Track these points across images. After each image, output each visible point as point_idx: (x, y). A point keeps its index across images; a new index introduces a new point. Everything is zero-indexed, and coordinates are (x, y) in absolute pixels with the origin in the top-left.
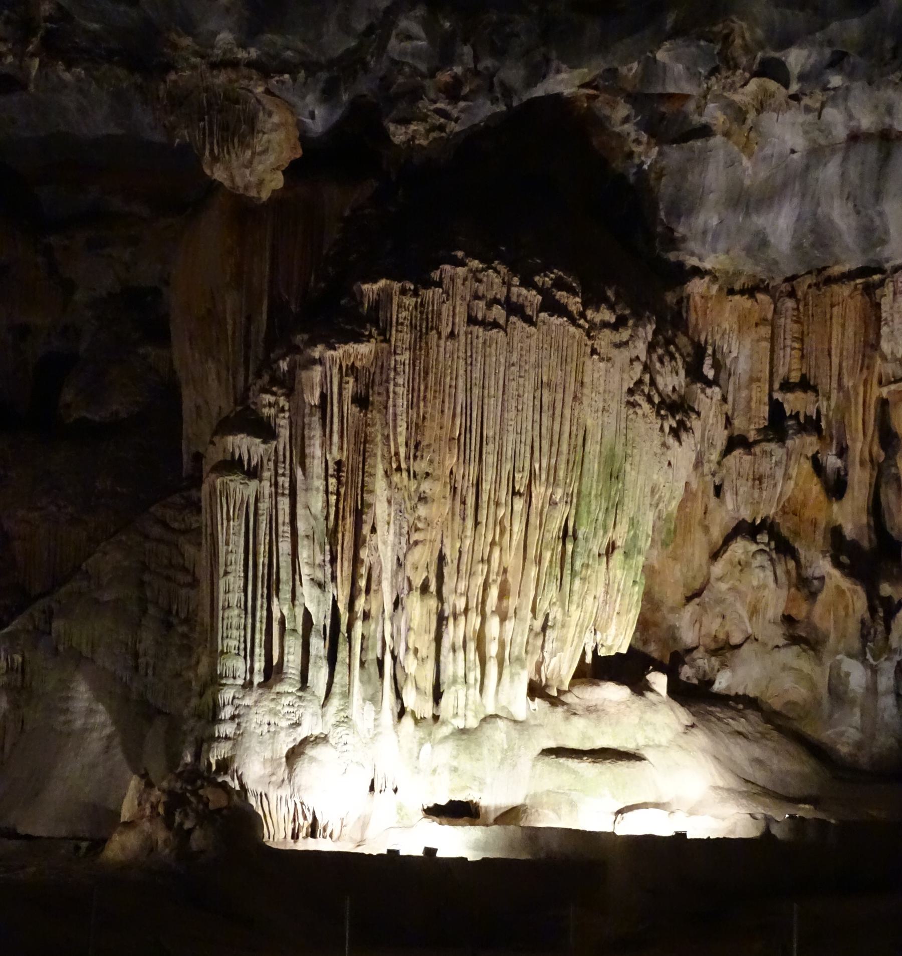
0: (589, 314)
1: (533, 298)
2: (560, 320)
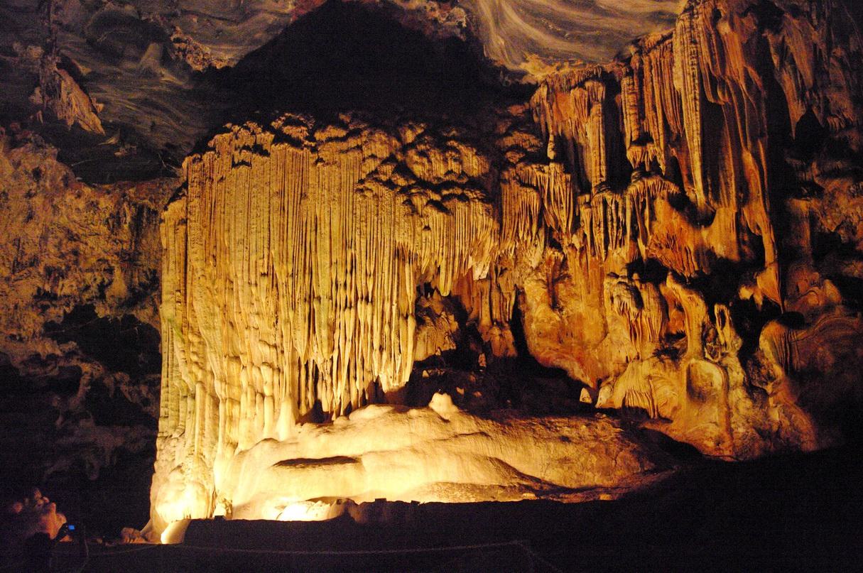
0: (318, 135)
1: (269, 137)
2: (282, 146)
